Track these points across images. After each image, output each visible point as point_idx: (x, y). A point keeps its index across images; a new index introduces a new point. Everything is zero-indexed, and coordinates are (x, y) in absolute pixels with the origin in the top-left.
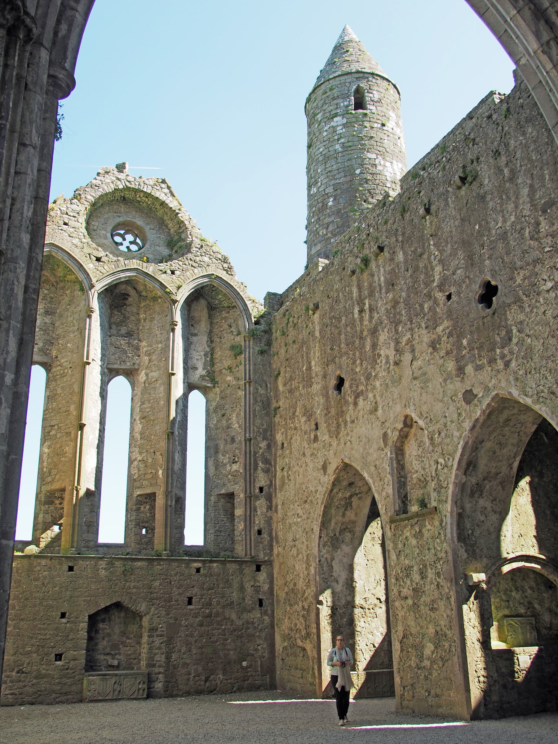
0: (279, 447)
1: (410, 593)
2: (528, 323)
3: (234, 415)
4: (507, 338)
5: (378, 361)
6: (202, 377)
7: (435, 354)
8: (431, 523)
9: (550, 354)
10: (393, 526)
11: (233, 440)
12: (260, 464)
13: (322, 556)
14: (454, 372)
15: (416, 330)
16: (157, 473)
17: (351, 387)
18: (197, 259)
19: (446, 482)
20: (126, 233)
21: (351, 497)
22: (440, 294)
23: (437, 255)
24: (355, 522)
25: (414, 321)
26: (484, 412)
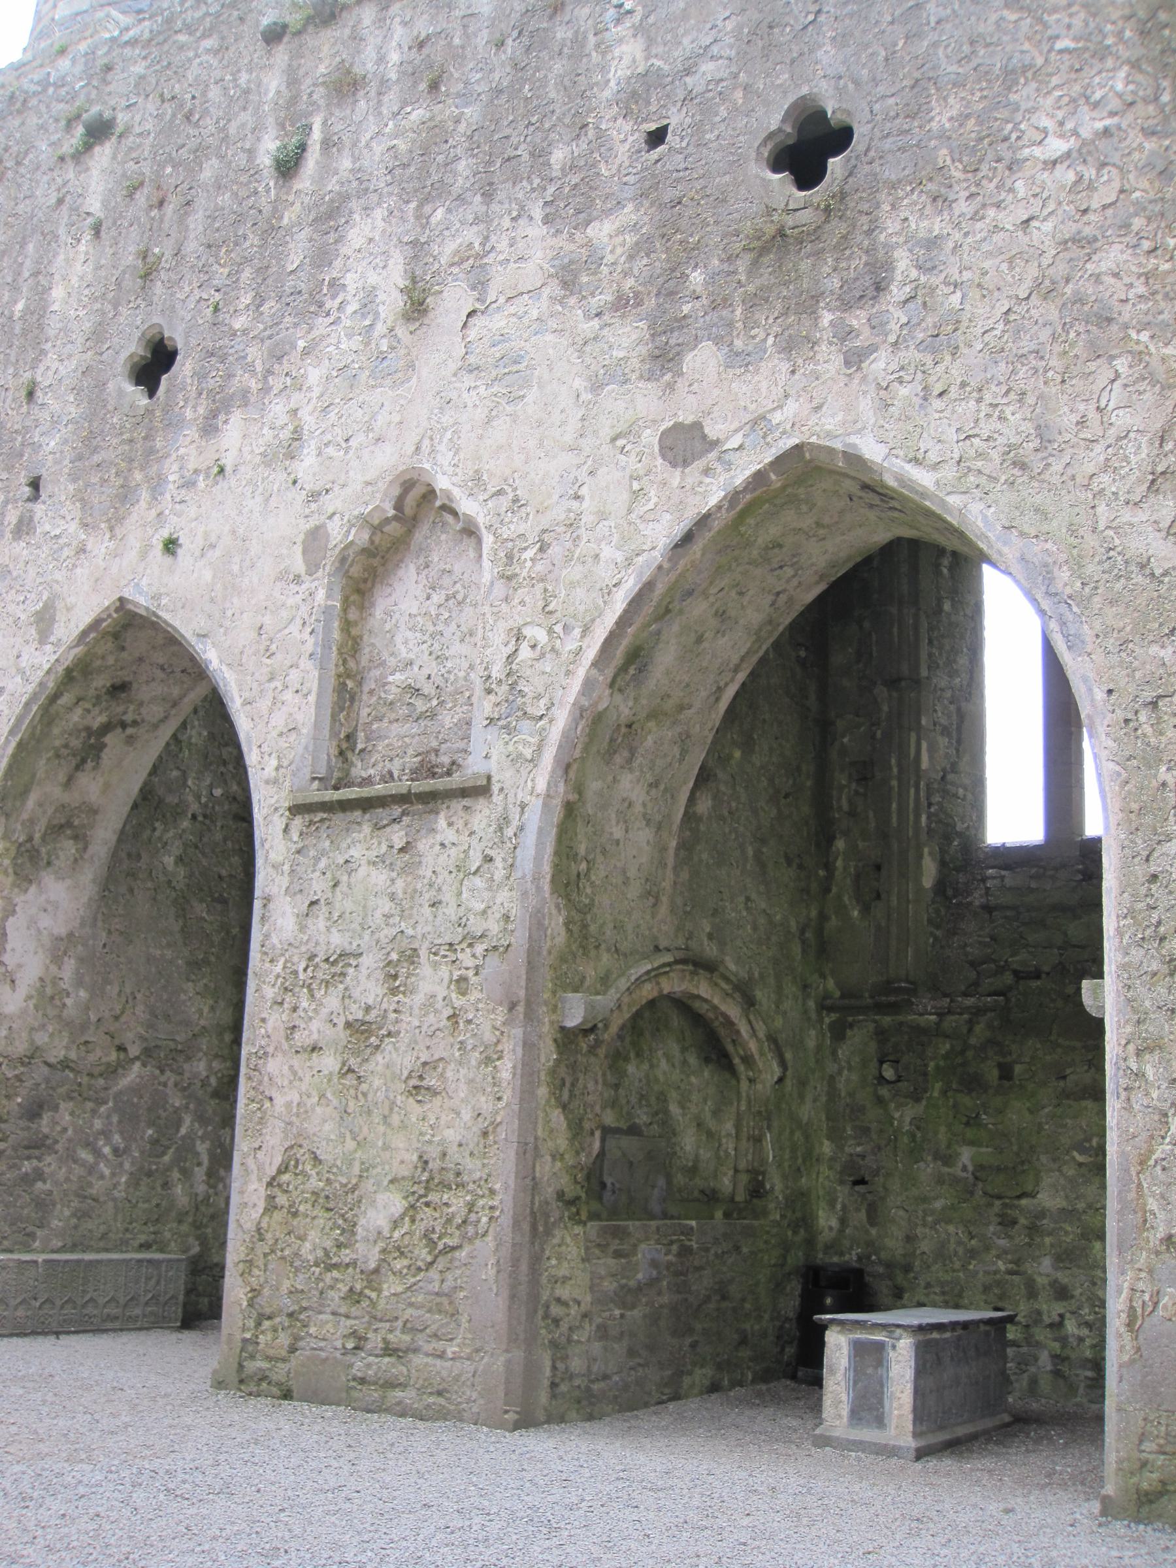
1: (342, 1034)
2: (957, 247)
4: (868, 281)
5: (328, 305)
7: (572, 301)
8: (460, 824)
9: (1026, 345)
10: (298, 822)
14: (635, 362)
15: (506, 222)
17: (200, 375)
19: (542, 702)
21: (106, 728)
22: (627, 126)
23: (629, 12)
24: (96, 812)
25: (501, 195)
26: (733, 497)
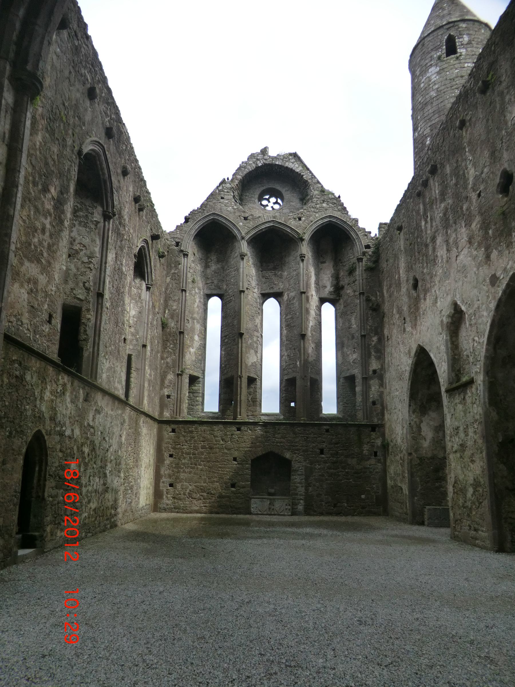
0: (386, 339)
3: (353, 318)
5: (437, 261)
6: (330, 293)
11: (353, 337)
12: (373, 353)
13: (412, 420)
16: (296, 364)
17: (422, 286)
18: (318, 206)
20: (269, 198)
26: (504, 292)
